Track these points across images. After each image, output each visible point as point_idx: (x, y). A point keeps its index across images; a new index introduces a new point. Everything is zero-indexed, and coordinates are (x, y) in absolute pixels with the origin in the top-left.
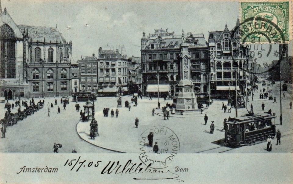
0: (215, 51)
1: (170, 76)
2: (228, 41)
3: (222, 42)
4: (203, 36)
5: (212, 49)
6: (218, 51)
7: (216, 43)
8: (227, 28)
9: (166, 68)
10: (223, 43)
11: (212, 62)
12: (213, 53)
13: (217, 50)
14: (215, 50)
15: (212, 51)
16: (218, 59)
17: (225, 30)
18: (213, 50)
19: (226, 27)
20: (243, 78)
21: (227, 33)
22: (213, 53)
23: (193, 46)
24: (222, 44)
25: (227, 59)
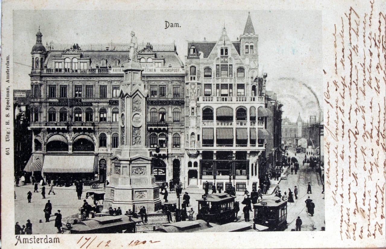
0: (198, 84)
1: (98, 135)
4: (175, 49)
11: (193, 108)
16: (205, 102)
20: (257, 144)
23: (150, 70)
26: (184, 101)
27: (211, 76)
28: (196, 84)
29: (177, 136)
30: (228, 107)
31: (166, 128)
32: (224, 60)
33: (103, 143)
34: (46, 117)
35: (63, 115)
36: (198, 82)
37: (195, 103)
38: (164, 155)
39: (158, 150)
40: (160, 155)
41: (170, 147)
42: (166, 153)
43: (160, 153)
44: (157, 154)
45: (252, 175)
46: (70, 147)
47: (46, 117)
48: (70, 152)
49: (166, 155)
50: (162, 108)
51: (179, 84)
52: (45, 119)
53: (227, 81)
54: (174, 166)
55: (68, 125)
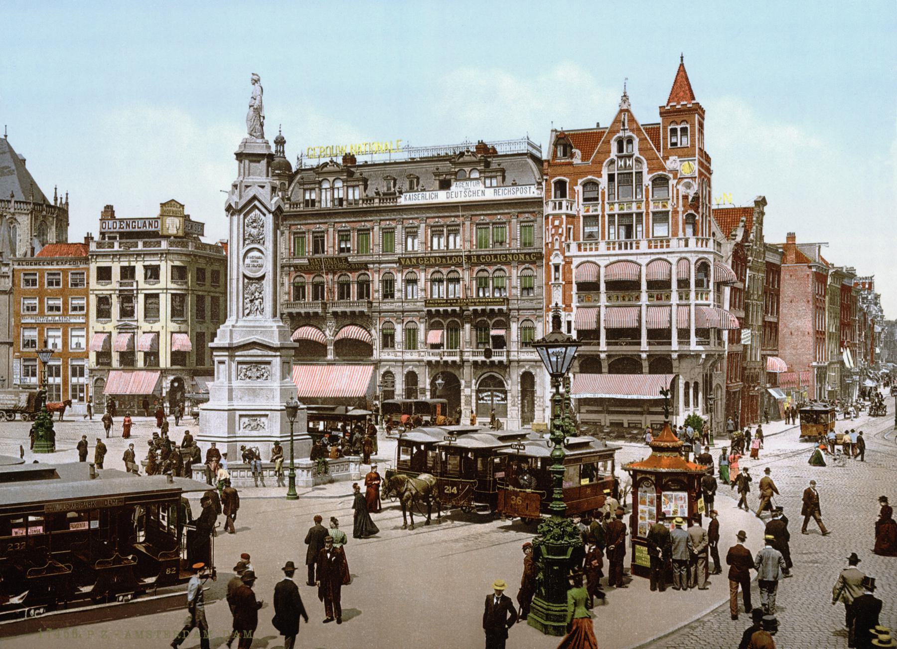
2: (634, 171)
3: (605, 173)
5: (560, 208)
6: (584, 217)
7: (580, 181)
8: (628, 111)
9: (364, 289)
10: (611, 178)
12: (564, 226)
13: (582, 213)
14: (574, 212)
15: (556, 216)
17: (617, 121)
18: (564, 210)
19: (625, 107)
21: (629, 133)
22: (561, 223)
24: (603, 181)
25: (623, 251)
26: (541, 253)
27: (596, 199)
28: (564, 217)
29: (529, 324)
30: (632, 262)
31: (504, 308)
32: (625, 163)
33: (388, 340)
34: (289, 293)
35: (318, 289)
36: (569, 212)
37: (562, 257)
38: (501, 362)
39: (488, 353)
40: (492, 362)
41: (514, 347)
42: (504, 359)
43: (493, 358)
44: (488, 361)
45: (687, 404)
46: (331, 348)
47: (289, 293)
48: (330, 357)
49: (505, 363)
50: (497, 270)
51: (532, 218)
52: (286, 297)
53: (630, 208)
54: (523, 384)
55: (324, 305)
